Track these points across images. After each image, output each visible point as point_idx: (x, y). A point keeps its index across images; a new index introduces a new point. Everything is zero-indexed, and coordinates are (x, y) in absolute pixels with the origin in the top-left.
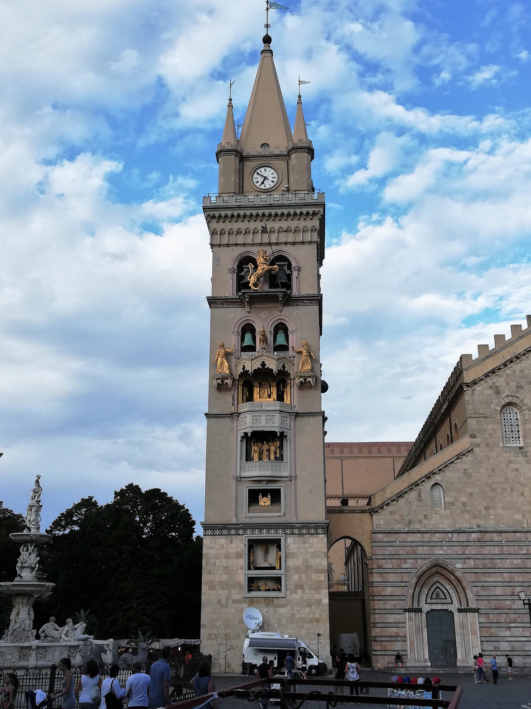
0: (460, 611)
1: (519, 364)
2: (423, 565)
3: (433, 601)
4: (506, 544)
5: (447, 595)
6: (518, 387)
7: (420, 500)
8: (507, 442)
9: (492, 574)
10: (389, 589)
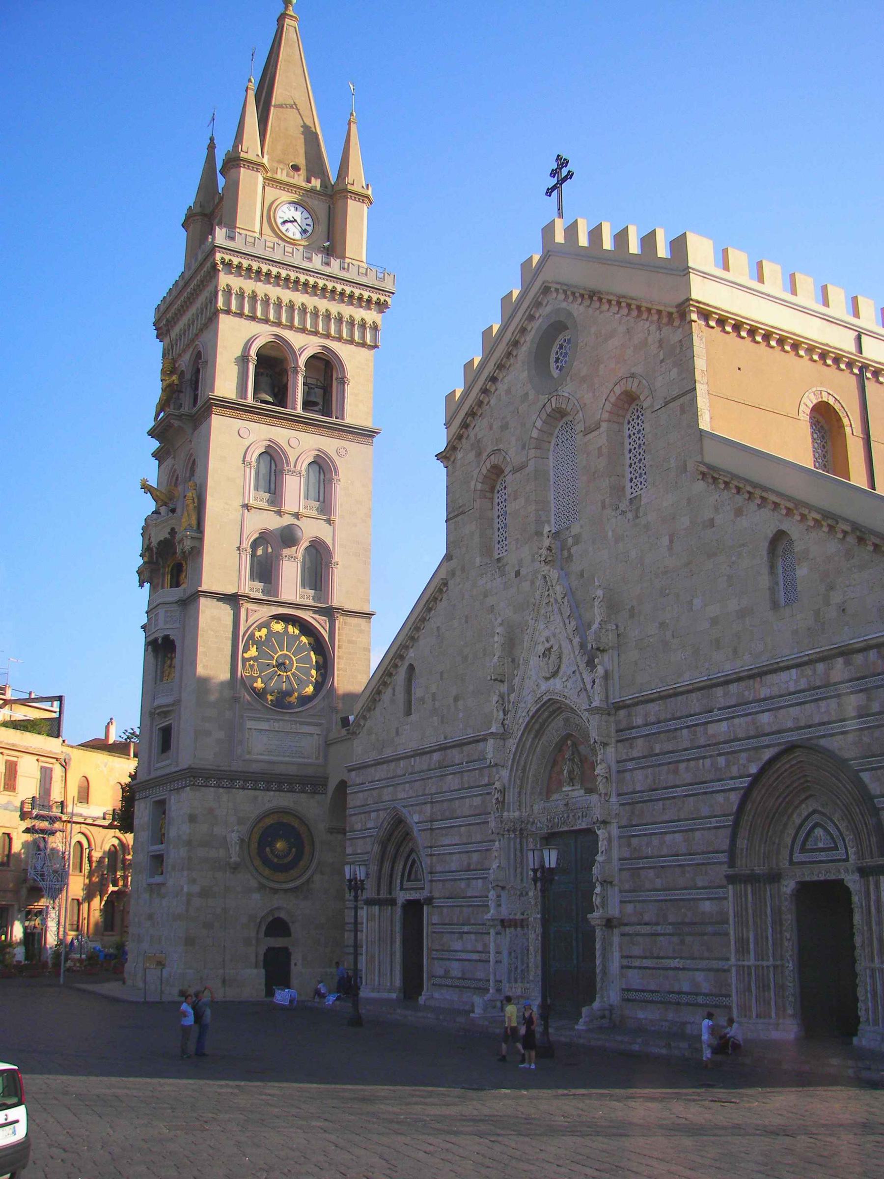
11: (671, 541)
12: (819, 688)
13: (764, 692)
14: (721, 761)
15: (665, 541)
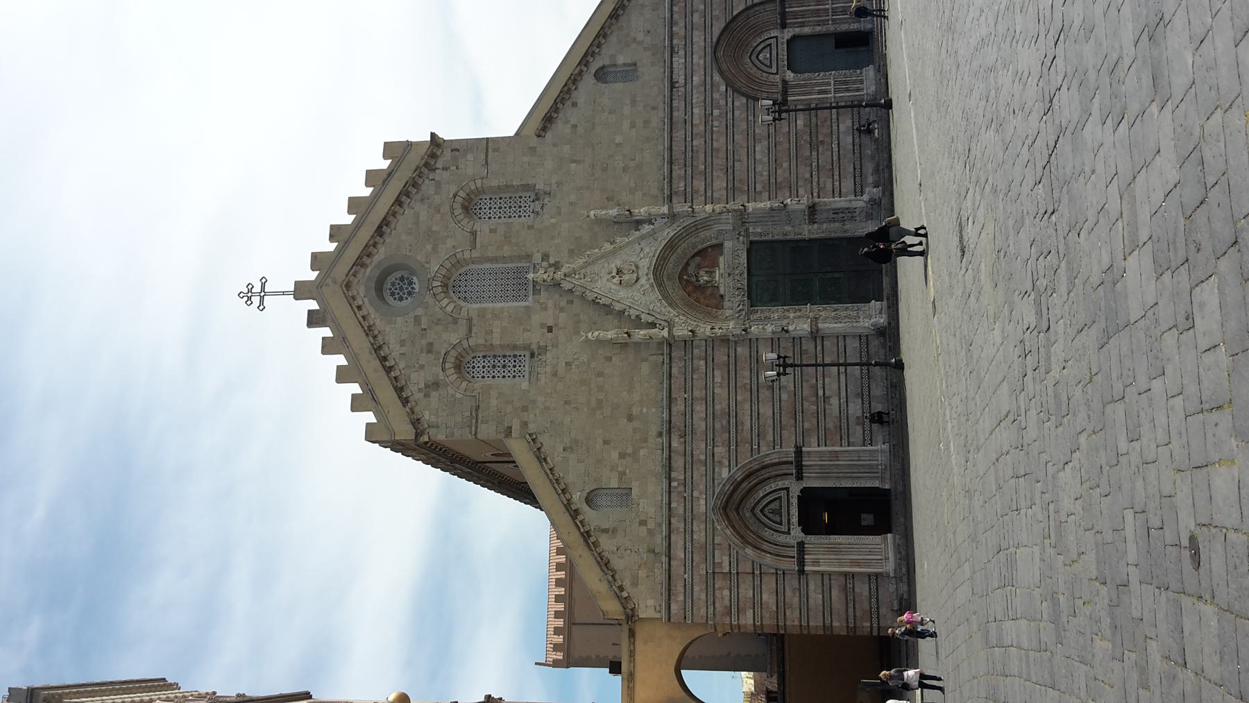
0: (800, 477)
1: (391, 347)
2: (724, 533)
3: (785, 520)
4: (689, 392)
5: (775, 496)
6: (429, 351)
7: (614, 531)
8: (521, 375)
9: (738, 417)
10: (765, 597)
11: (574, 161)
12: (686, 42)
13: (682, 81)
14: (716, 112)
15: (573, 166)
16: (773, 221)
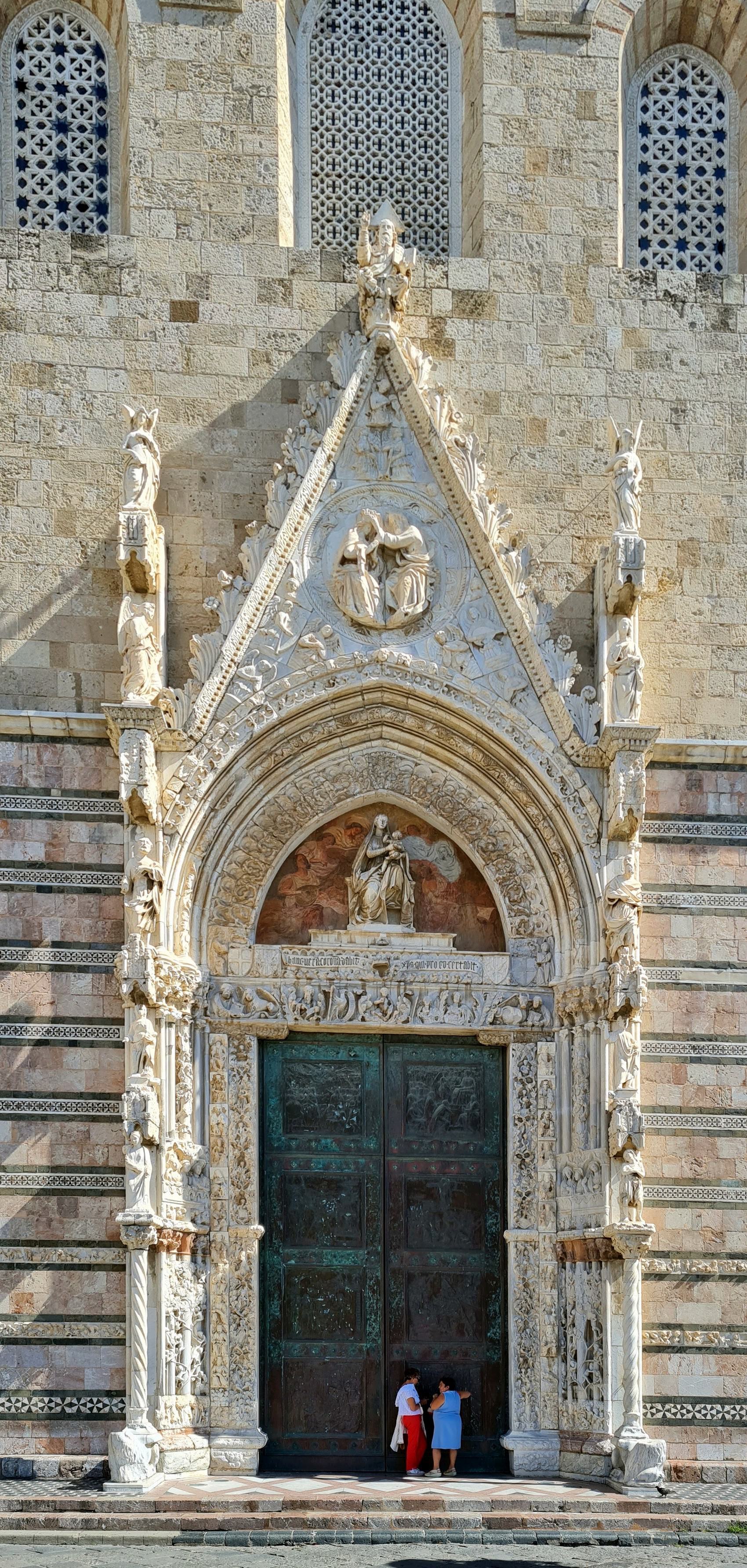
16: (571, 1119)
